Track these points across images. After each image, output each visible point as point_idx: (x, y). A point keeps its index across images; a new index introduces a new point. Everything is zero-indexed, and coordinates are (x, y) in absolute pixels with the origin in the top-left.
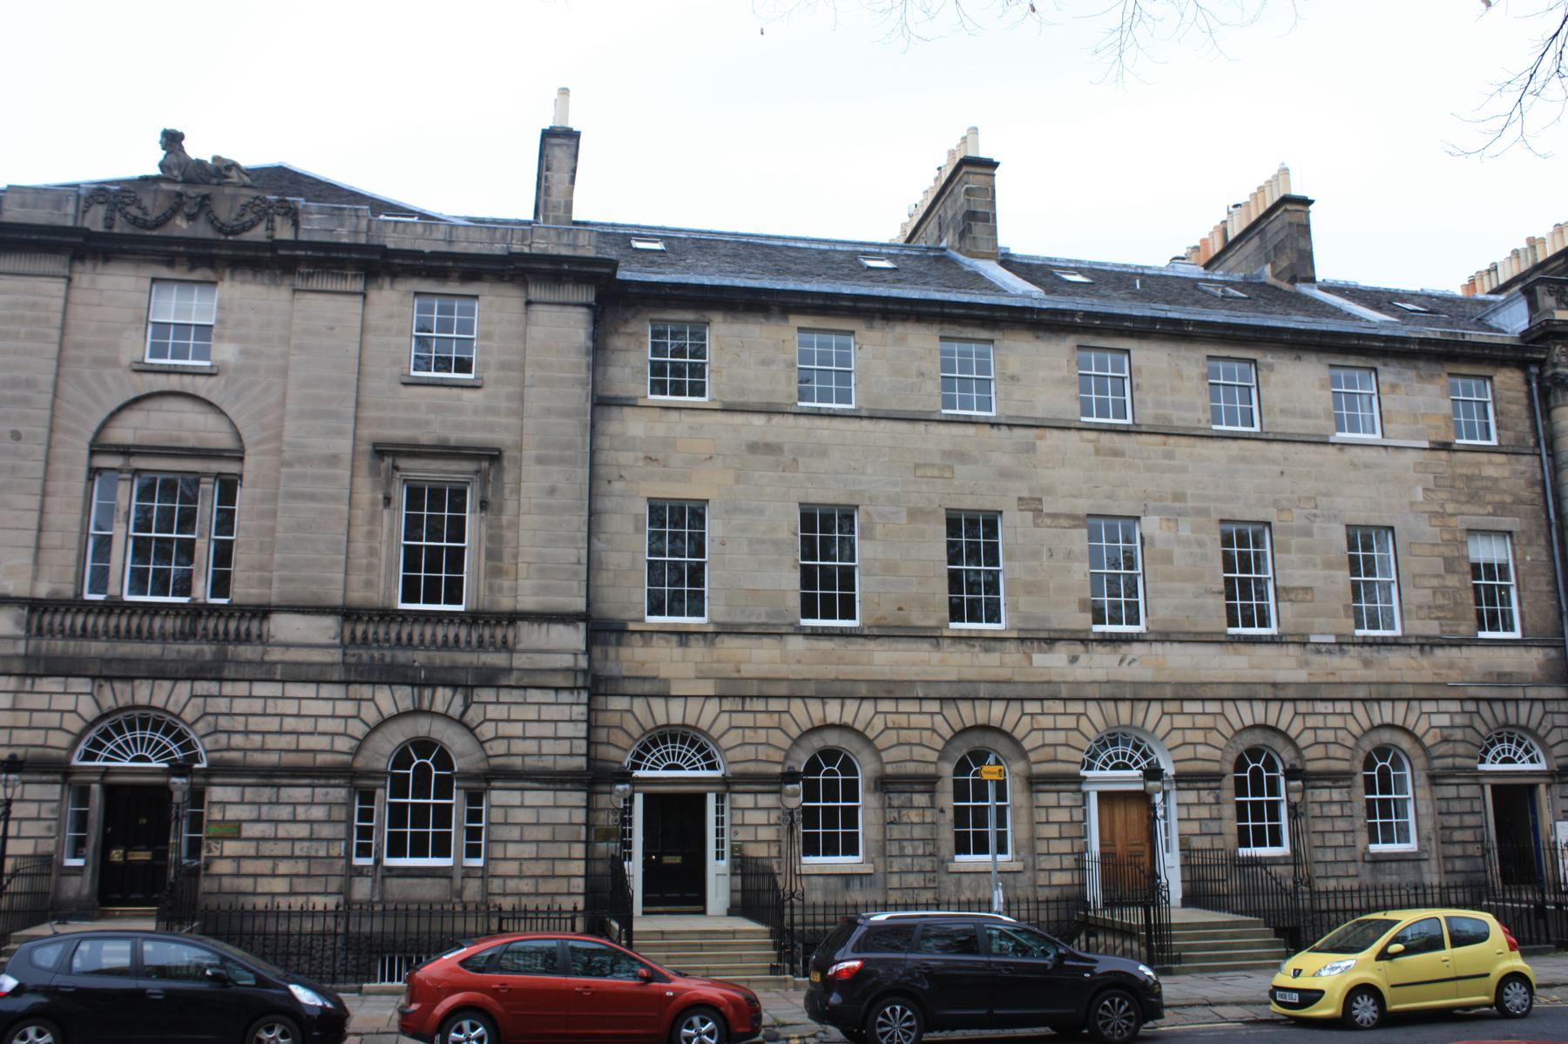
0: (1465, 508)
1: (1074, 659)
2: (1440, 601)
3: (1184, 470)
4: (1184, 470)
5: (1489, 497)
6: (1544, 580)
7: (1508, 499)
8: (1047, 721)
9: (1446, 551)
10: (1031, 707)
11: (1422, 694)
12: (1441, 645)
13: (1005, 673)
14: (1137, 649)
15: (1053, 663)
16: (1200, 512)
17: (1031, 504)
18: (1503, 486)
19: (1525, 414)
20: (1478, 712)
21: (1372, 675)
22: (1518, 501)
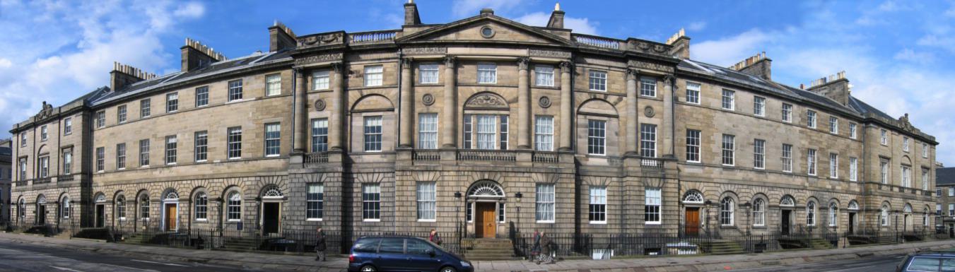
0: (265, 117)
1: (160, 172)
2: (253, 147)
3: (187, 120)
4: (187, 120)
5: (274, 112)
6: (288, 136)
7: (280, 111)
8: (154, 187)
9: (257, 131)
10: (152, 184)
11: (243, 175)
12: (252, 160)
13: (148, 177)
14: (174, 168)
15: (157, 173)
16: (190, 131)
17: (155, 136)
18: (278, 107)
19: (291, 82)
20: (260, 180)
21: (230, 171)
22: (283, 111)
